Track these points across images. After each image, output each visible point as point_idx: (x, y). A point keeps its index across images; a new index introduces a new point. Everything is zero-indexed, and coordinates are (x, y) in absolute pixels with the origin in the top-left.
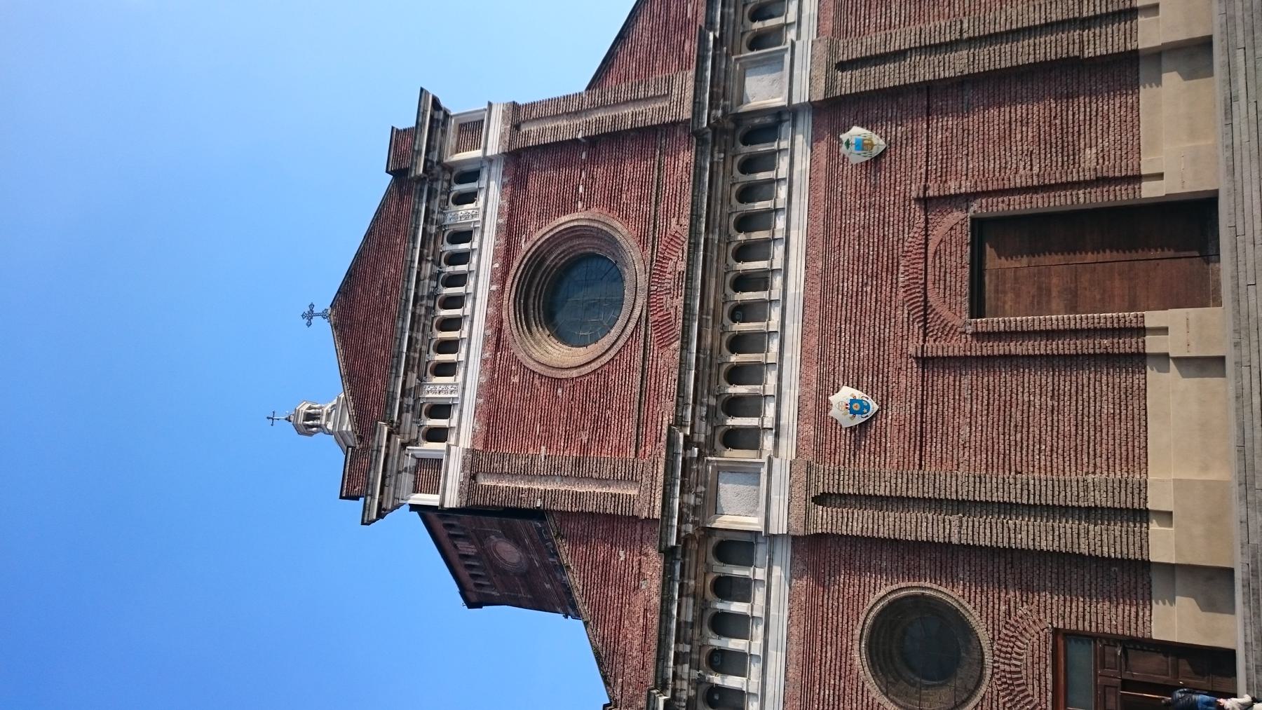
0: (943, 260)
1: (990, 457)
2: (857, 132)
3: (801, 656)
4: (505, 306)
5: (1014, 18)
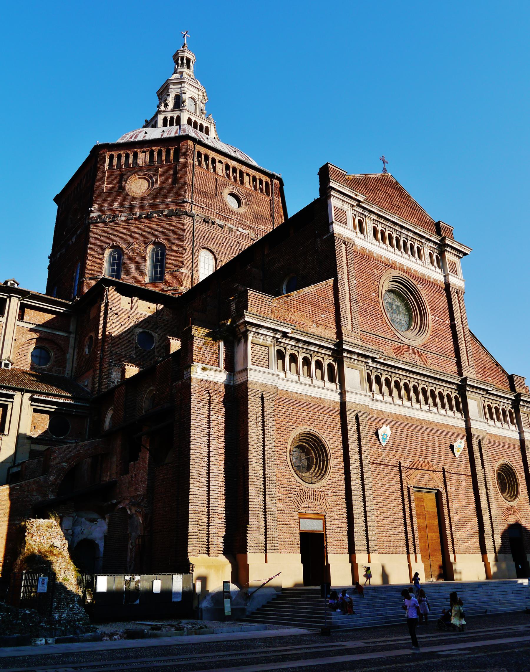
3: (302, 401)
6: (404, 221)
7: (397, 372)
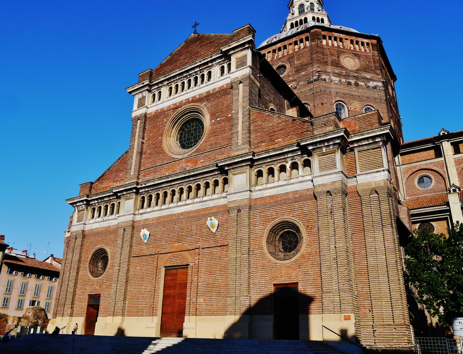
2: (216, 222)
4: (185, 106)
6: (184, 67)
7: (161, 187)
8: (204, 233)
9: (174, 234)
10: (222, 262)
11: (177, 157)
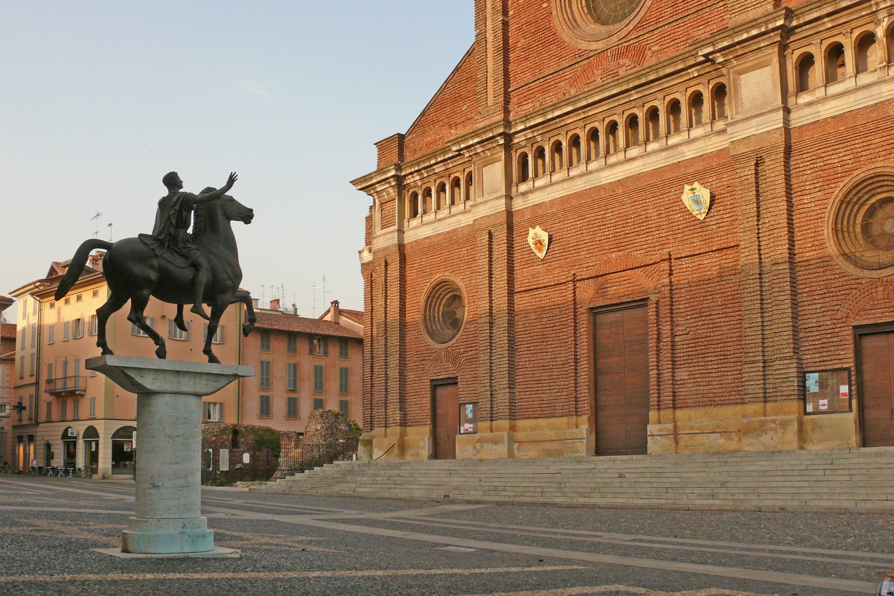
0: (625, 282)
1: (522, 333)
5: (782, 307)
8: (679, 223)
9: (607, 233)
10: (727, 286)
11: (594, 46)
